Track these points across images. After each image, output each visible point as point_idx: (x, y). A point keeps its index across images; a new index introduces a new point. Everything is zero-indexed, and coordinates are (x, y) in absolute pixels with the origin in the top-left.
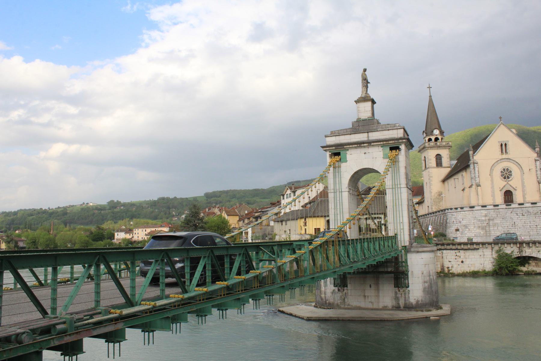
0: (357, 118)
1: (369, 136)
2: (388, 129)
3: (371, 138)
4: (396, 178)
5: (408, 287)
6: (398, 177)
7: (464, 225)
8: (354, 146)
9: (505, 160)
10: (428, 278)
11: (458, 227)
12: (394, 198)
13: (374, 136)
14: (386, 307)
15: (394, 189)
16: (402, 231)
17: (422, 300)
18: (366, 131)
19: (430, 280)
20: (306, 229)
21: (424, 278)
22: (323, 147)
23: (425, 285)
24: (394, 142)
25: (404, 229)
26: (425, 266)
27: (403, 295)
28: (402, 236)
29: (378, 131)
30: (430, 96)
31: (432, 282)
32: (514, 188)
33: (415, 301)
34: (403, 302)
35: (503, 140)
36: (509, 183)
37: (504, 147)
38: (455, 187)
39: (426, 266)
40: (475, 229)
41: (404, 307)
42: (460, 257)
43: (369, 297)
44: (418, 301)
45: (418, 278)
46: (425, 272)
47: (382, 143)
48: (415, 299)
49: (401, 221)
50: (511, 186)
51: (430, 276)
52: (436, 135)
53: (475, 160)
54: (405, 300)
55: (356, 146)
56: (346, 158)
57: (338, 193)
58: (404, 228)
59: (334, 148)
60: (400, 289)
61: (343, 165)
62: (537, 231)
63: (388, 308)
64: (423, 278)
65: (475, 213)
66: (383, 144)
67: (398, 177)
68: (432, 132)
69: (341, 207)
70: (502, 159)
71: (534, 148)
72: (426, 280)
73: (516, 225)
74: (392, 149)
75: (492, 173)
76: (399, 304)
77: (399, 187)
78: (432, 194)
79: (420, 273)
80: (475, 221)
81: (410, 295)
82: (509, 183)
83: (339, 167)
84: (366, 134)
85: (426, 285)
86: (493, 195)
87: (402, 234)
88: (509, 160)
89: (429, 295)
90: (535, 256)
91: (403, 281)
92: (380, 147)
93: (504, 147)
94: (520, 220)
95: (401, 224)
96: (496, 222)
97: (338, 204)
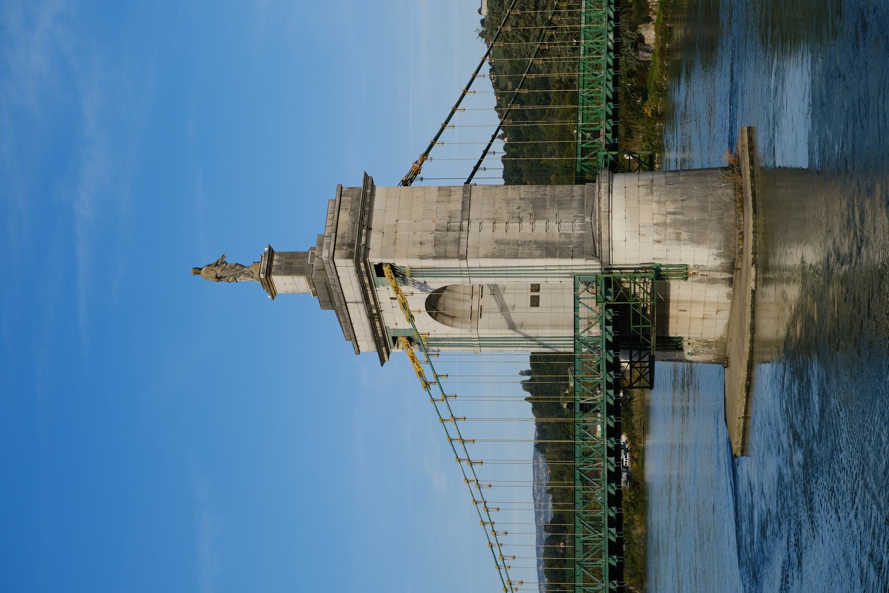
10: (669, 230)
17: (718, 248)
18: (344, 307)
19: (675, 224)
21: (670, 239)
22: (382, 361)
23: (685, 240)
26: (644, 235)
27: (705, 273)
34: (719, 273)
39: (641, 233)
41: (732, 273)
44: (719, 255)
45: (667, 250)
46: (657, 237)
47: (369, 292)
51: (665, 225)
54: (717, 271)
55: (378, 324)
64: (669, 242)
72: (673, 237)
76: (722, 279)
79: (657, 246)
81: (705, 264)
85: (684, 235)
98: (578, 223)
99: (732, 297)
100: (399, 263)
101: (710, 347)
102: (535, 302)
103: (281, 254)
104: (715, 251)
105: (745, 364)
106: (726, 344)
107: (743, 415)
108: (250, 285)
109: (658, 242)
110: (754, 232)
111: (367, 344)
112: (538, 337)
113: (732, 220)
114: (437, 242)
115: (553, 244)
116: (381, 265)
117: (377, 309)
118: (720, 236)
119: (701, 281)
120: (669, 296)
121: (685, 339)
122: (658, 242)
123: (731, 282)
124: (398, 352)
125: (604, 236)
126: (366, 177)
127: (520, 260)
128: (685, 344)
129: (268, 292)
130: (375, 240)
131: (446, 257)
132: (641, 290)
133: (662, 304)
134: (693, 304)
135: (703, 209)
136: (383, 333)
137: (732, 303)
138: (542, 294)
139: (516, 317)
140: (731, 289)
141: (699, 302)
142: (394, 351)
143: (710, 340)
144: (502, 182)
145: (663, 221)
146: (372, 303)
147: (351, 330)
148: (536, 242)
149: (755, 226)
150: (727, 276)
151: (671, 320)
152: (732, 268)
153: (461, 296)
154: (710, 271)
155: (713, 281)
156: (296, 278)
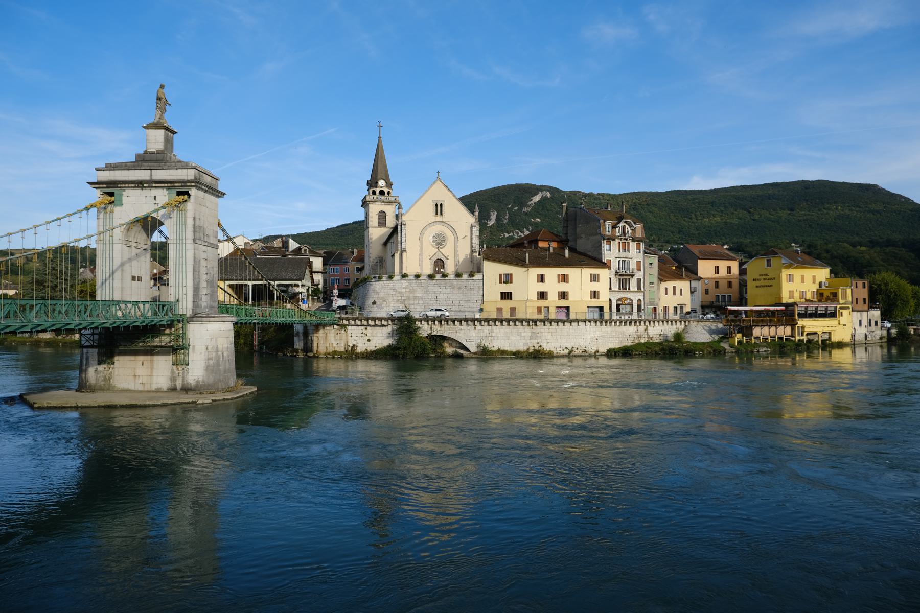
0: (145, 149)
1: (153, 175)
2: (175, 168)
3: (154, 178)
4: (181, 231)
5: (188, 365)
6: (184, 231)
7: (382, 298)
8: (130, 185)
9: (439, 223)
10: (214, 354)
11: (376, 299)
12: (178, 256)
13: (160, 174)
14: (160, 389)
15: (178, 244)
16: (184, 296)
17: (203, 381)
18: (148, 168)
19: (218, 357)
21: (209, 354)
23: (208, 363)
24: (180, 185)
25: (187, 295)
26: (211, 340)
27: (181, 375)
28: (184, 303)
30: (380, 137)
31: (220, 358)
32: (445, 257)
33: (194, 381)
34: (181, 382)
35: (439, 199)
36: (441, 250)
37: (439, 209)
39: (213, 339)
40: (393, 303)
41: (181, 389)
42: (366, 335)
43: (141, 377)
45: (201, 353)
46: (210, 348)
47: (166, 185)
48: (195, 379)
49: (184, 285)
50: (442, 254)
51: (217, 351)
52: (382, 187)
53: (404, 221)
54: (183, 381)
55: (133, 185)
56: (122, 201)
57: (108, 246)
58: (187, 293)
60: (178, 367)
61: (117, 209)
62: (460, 307)
63: (162, 390)
64: (207, 354)
65: (394, 284)
67: (184, 231)
68: (377, 183)
69: (111, 264)
70: (435, 222)
71: (472, 211)
73: (438, 300)
74: (179, 193)
75: (422, 238)
76: (175, 385)
77: (184, 242)
78: (371, 259)
79: (204, 348)
80: (394, 293)
81: (190, 374)
82: (441, 250)
83: (112, 212)
84: (149, 171)
85: (211, 362)
86: (421, 264)
87: (184, 300)
88: (443, 224)
89: (214, 375)
90: (447, 336)
91: (183, 358)
92: (165, 190)
93: (439, 209)
94: (443, 294)
95: (184, 288)
96: (417, 295)
97: (108, 259)
98: (205, 304)
99: (158, 391)
100: (190, 206)
101: (105, 380)
102: (133, 278)
103: (173, 137)
104: (201, 379)
105: (133, 403)
106: (109, 389)
107: (80, 405)
108: (153, 117)
109: (207, 348)
110: (224, 400)
112: (113, 279)
113: (220, 387)
114: (200, 227)
115: (199, 291)
116: (189, 195)
117: (145, 187)
118: (211, 380)
119: (173, 372)
120: (158, 355)
121: (112, 366)
122: (207, 348)
123: (173, 389)
124: (96, 195)
125: (212, 319)
126: (224, 194)
127: (192, 273)
128: (105, 366)
129: (147, 125)
130: (201, 193)
131: (194, 232)
132: (164, 339)
133: (150, 352)
134: (150, 370)
135: (225, 372)
136: (120, 187)
137: (153, 392)
138: (136, 282)
139: (127, 267)
140: (165, 390)
141: (152, 372)
142: (98, 193)
143: (111, 380)
144: (403, 273)
145: (219, 350)
146: (154, 185)
147: (125, 168)
148: (199, 281)
149: (228, 400)
150: (179, 386)
151: (134, 357)
152: (186, 389)
153: (136, 236)
154: (183, 377)
155: (173, 379)
156: (163, 143)
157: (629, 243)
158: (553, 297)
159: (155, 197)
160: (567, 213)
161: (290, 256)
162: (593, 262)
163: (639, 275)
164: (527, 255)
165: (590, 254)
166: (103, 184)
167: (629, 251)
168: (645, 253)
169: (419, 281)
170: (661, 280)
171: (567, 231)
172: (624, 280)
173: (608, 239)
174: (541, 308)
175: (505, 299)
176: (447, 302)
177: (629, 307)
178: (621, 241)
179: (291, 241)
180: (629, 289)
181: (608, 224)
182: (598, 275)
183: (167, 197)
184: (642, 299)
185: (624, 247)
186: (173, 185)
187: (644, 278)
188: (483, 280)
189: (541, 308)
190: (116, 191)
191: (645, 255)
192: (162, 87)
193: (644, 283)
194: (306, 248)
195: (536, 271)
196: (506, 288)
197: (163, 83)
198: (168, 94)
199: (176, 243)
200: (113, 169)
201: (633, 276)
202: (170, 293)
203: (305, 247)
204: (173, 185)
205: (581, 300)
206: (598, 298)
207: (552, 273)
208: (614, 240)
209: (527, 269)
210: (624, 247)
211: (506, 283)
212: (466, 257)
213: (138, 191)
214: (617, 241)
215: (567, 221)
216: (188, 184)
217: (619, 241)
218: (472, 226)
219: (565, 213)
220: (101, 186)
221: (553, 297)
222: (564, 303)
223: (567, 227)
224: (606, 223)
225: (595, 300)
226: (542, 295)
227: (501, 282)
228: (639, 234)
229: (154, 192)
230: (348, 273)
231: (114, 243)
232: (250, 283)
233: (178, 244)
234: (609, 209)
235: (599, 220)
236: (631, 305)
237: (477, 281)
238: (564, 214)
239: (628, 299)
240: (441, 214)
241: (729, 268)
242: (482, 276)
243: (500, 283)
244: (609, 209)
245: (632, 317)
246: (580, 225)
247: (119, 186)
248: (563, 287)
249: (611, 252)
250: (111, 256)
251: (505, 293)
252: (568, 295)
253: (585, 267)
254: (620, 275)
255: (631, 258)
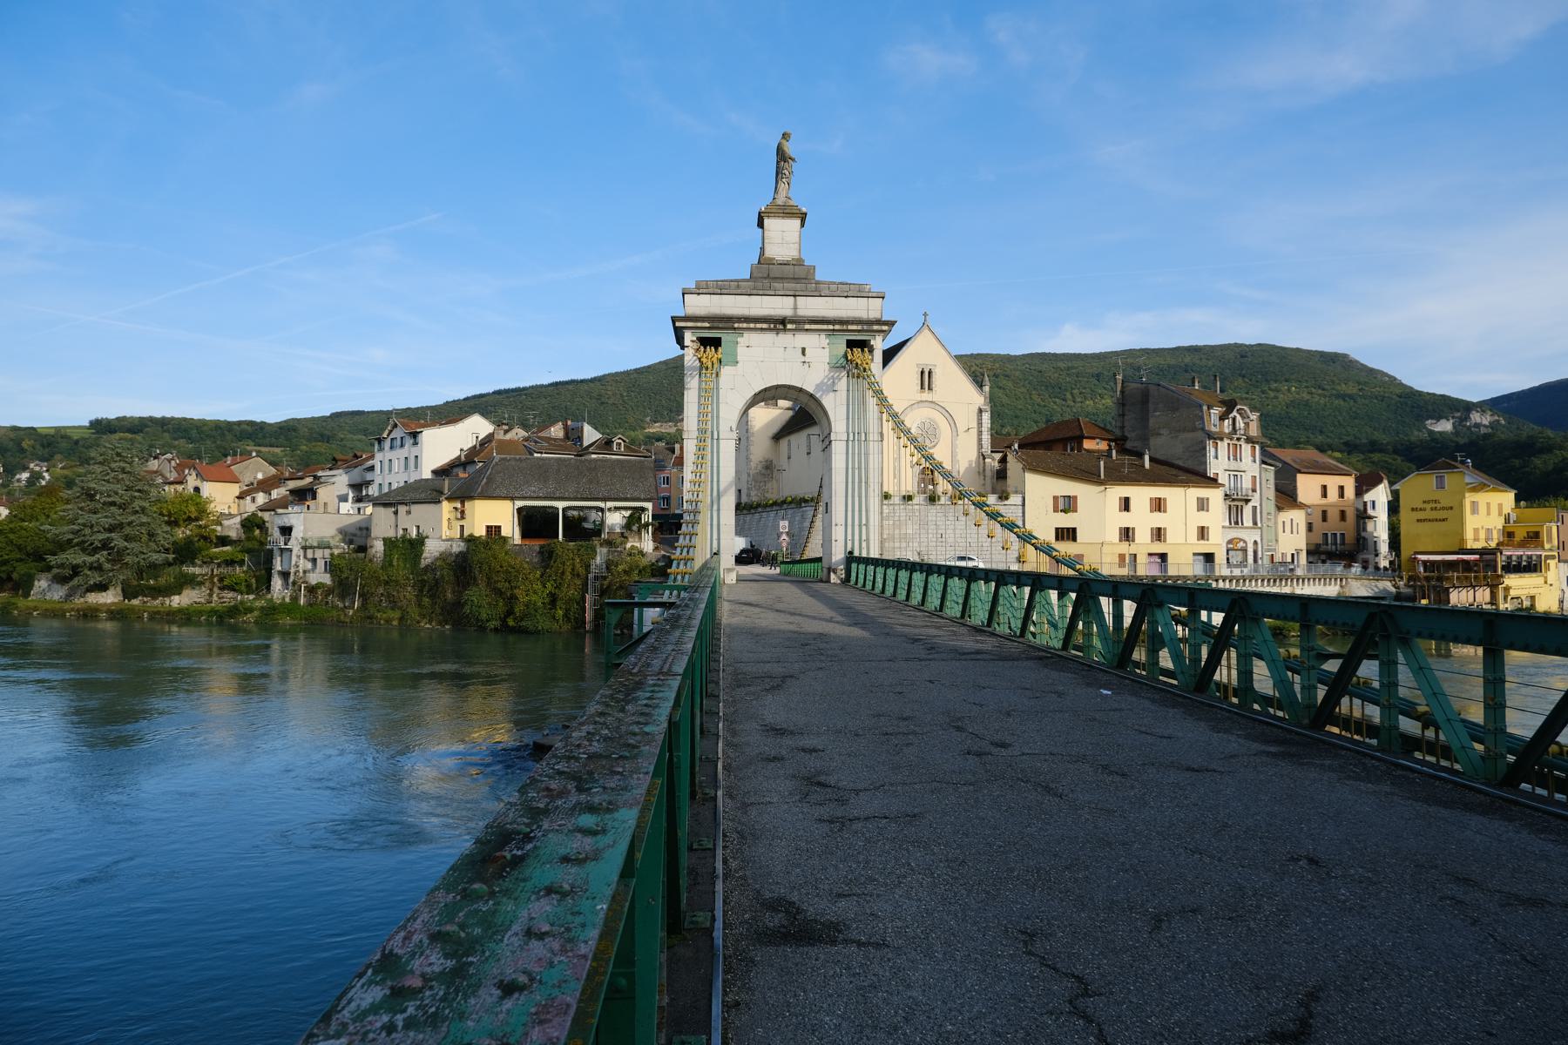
3: (802, 312)
8: (759, 326)
16: (864, 544)
20: (462, 527)
24: (859, 327)
29: (821, 296)
38: (809, 454)
47: (831, 327)
55: (765, 326)
56: (736, 356)
59: (707, 325)
66: (834, 330)
70: (921, 401)
71: (980, 385)
88: (933, 405)
95: (864, 528)
111: (702, 305)
112: (719, 510)
136: (739, 328)
146: (807, 327)
157: (1240, 445)
158: (1143, 536)
159: (804, 350)
160: (1122, 392)
161: (594, 456)
162: (1194, 478)
163: (1255, 502)
164: (1102, 463)
165: (1180, 463)
166: (703, 321)
167: (1241, 460)
168: (1264, 462)
169: (910, 507)
170: (1279, 508)
171: (1123, 422)
172: (1236, 504)
173: (1215, 439)
174: (1125, 555)
175: (1063, 539)
176: (961, 544)
177: (1240, 553)
178: (1231, 442)
179: (587, 428)
180: (1242, 524)
181: (1216, 412)
182: (1208, 499)
183: (827, 350)
184: (1259, 541)
185: (1235, 455)
186: (845, 327)
187: (1261, 505)
188: (1023, 505)
189: (1125, 555)
190: (726, 337)
191: (1264, 466)
192: (785, 136)
193: (1261, 513)
194: (620, 441)
195: (1118, 492)
196: (1065, 521)
197: (788, 131)
198: (790, 148)
199: (847, 441)
200: (719, 291)
201: (1247, 501)
202: (833, 538)
203: (620, 438)
204: (845, 327)
205: (1184, 542)
206: (1208, 540)
207: (1141, 495)
208: (1222, 439)
209: (1103, 488)
210: (1235, 455)
211: (1064, 511)
212: (970, 465)
213: (769, 337)
214: (1226, 441)
215: (1123, 405)
216: (875, 327)
217: (1229, 441)
218: (980, 411)
219: (1121, 391)
220: (699, 324)
221: (1143, 536)
222: (1158, 548)
223: (1123, 415)
224: (1212, 411)
225: (1202, 542)
226: (1127, 534)
227: (1056, 510)
228: (1254, 430)
229: (802, 339)
230: (666, 486)
231: (721, 437)
232: (560, 505)
233: (850, 443)
234: (1197, 388)
235: (1201, 406)
236: (1244, 550)
237: (1013, 507)
238: (1118, 393)
239: (1241, 540)
240: (930, 388)
241: (1342, 488)
242: (1020, 499)
243: (1054, 511)
244: (1197, 388)
245: (1246, 571)
246: (1158, 413)
247: (736, 325)
248: (1158, 520)
249: (1218, 462)
250: (715, 464)
251: (1063, 529)
252: (1165, 535)
253: (1193, 487)
254: (1234, 500)
255: (1244, 472)
